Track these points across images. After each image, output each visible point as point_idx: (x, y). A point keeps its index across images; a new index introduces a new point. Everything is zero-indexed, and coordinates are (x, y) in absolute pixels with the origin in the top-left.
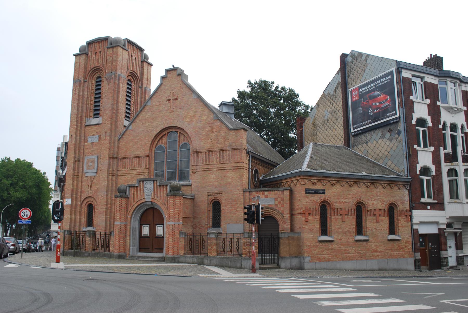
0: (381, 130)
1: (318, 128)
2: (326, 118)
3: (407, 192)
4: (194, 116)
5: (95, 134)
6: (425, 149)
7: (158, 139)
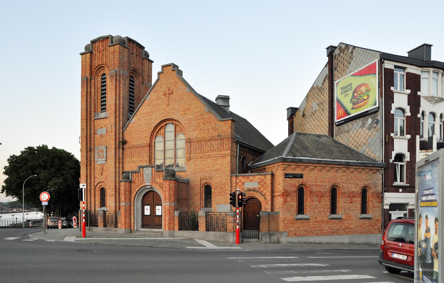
0: (361, 119)
1: (307, 118)
2: (314, 109)
3: (381, 176)
4: (188, 109)
5: (103, 127)
6: (402, 137)
7: (157, 130)
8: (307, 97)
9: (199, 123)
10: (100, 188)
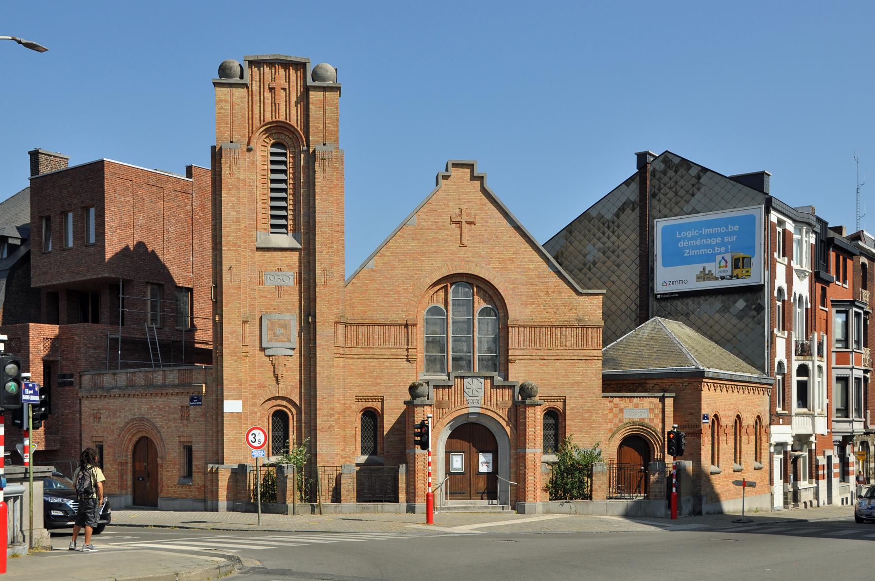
4: (512, 261)
8: (569, 229)
9: (535, 291)
10: (278, 408)
